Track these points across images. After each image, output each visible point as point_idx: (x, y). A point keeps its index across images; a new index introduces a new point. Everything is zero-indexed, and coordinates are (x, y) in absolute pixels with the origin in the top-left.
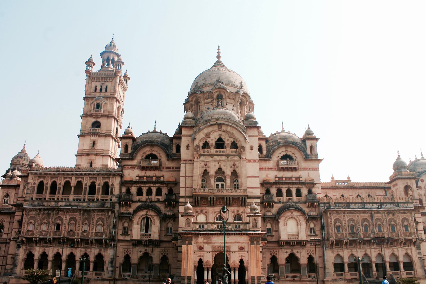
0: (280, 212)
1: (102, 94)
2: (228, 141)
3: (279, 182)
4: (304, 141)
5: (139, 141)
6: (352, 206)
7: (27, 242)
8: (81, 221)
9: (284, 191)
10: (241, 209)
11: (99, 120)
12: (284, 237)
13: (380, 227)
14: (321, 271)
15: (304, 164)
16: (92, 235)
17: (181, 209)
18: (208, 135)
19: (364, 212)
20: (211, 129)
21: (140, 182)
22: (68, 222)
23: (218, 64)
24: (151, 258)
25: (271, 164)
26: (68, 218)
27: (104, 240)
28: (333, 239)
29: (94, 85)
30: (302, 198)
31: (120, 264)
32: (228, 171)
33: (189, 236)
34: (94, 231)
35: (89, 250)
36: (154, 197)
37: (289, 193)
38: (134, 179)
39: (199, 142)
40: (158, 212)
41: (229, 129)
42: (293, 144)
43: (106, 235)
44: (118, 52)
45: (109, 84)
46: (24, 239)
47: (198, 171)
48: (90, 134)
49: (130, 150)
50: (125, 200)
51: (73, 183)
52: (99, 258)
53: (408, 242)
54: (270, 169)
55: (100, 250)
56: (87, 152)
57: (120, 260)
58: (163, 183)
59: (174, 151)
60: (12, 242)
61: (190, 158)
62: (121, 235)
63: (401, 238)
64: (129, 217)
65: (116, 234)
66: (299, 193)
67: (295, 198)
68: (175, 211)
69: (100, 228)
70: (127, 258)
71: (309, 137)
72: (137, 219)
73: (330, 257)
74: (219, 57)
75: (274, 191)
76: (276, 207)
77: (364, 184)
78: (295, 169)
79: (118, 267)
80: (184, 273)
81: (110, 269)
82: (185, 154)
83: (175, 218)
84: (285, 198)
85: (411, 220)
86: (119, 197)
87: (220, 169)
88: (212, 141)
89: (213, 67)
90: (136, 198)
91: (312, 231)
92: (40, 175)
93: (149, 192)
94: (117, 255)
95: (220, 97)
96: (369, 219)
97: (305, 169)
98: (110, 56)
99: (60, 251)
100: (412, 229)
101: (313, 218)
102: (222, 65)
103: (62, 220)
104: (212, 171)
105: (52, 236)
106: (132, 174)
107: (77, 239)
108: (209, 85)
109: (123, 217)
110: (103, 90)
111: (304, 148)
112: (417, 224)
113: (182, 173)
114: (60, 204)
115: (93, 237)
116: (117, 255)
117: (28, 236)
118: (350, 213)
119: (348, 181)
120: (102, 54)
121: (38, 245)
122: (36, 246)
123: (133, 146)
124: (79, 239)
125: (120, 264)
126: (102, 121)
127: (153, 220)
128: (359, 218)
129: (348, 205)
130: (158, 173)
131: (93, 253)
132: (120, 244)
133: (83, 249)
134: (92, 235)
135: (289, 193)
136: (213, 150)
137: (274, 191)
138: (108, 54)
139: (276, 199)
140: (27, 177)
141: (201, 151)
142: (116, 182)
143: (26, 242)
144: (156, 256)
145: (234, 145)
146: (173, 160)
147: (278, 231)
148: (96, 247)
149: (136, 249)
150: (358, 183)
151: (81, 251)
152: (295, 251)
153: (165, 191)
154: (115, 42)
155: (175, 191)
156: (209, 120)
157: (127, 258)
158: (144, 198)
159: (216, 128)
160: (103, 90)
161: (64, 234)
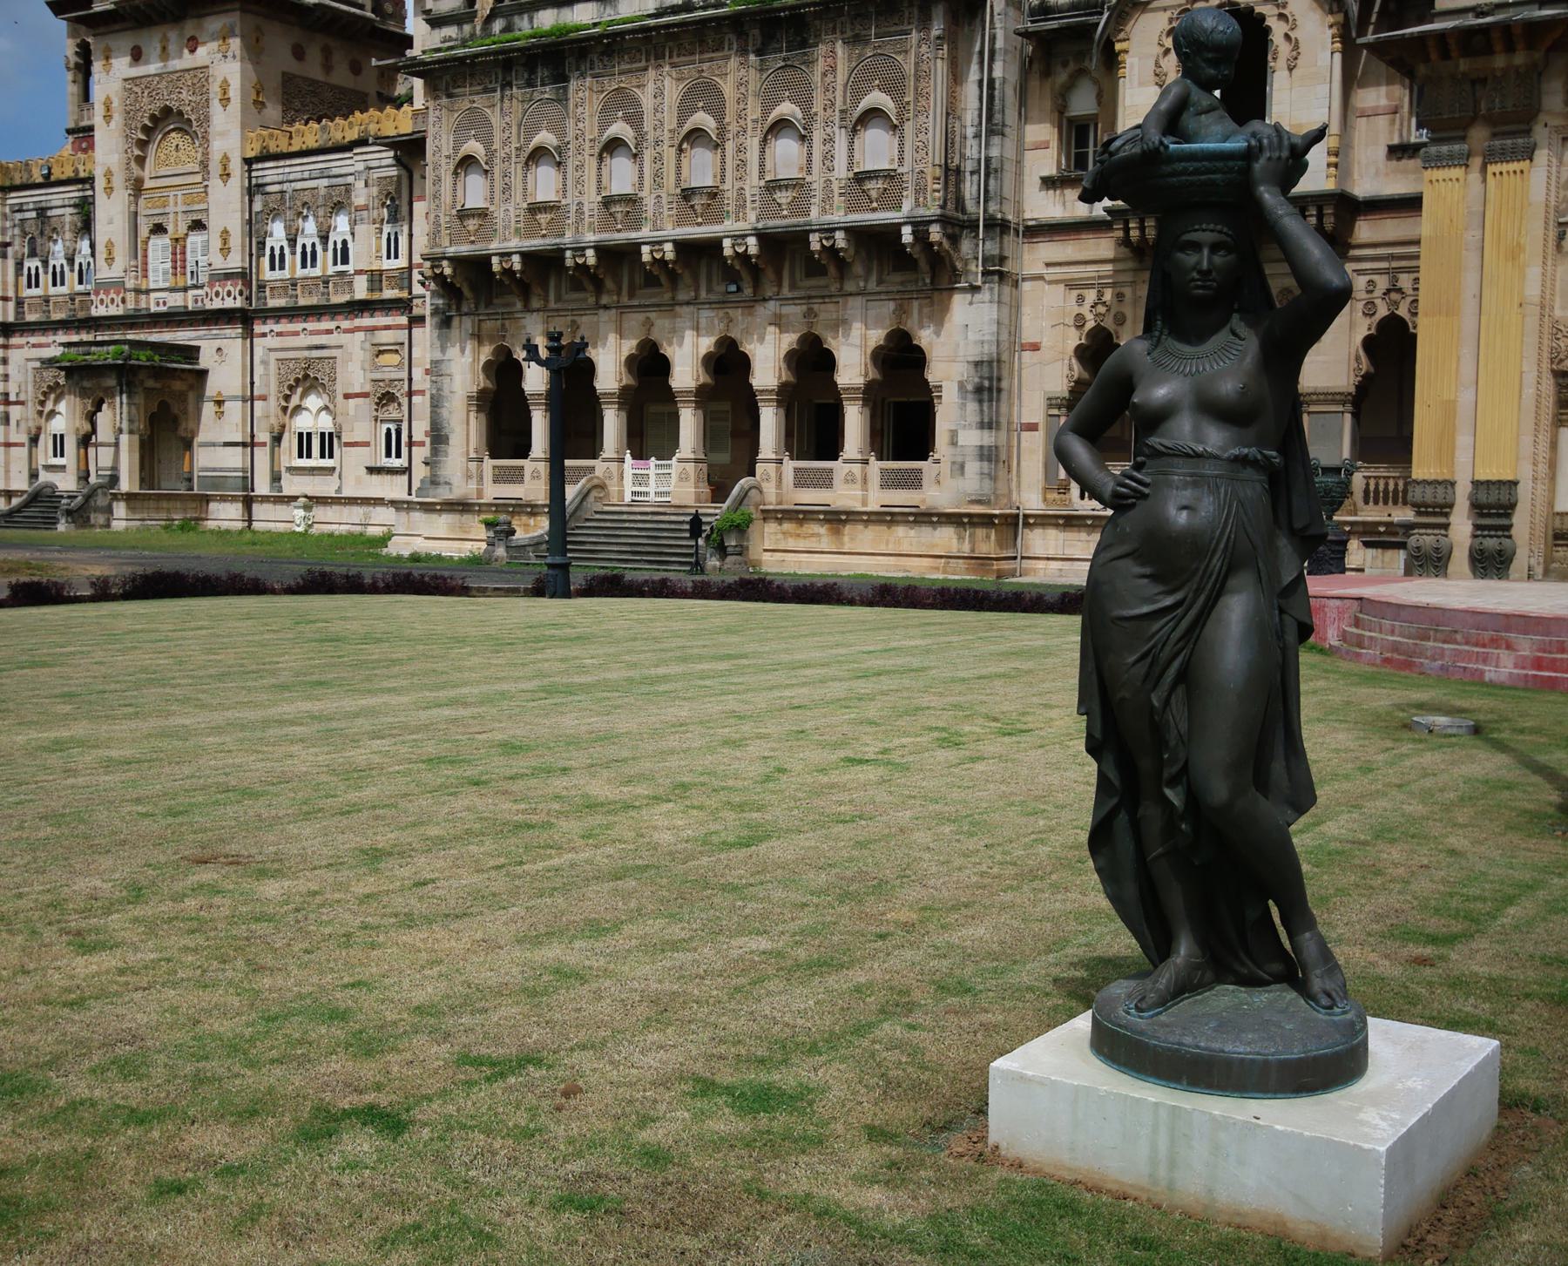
7: (473, 288)
8: (754, 111)
16: (827, 199)
22: (670, 121)
26: (673, 90)
27: (907, 231)
31: (1052, 402)
33: (1499, 61)
34: (841, 171)
35: (827, 312)
43: (920, 190)
46: (448, 271)
52: (901, 361)
55: (902, 311)
57: (1047, 375)
62: (1049, 183)
65: (1008, 177)
69: (877, 150)
79: (1033, 427)
80: (1446, 448)
81: (972, 438)
94: (1028, 336)
103: (635, 120)
105: (591, 237)
107: (740, 237)
115: (839, 216)
116: (1028, 336)
117: (464, 249)
121: (535, 303)
122: (527, 309)
124: (752, 241)
125: (1052, 402)
127: (1277, 29)
132: (1034, 258)
133: (794, 311)
134: (827, 199)
143: (467, 292)
148: (872, 286)
151: (779, 322)
161: (658, 214)
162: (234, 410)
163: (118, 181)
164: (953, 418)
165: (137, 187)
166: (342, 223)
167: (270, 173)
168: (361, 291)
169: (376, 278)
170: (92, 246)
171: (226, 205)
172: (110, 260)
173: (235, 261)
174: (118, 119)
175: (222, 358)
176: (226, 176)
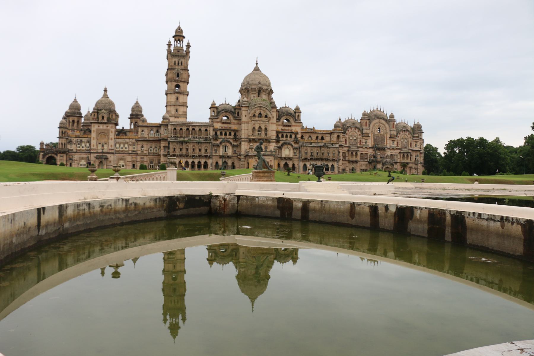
0: (282, 145)
1: (180, 68)
2: (264, 115)
3: (282, 132)
4: (295, 112)
5: (220, 109)
6: (313, 144)
9: (285, 135)
10: (267, 144)
11: (179, 84)
12: (283, 156)
13: (323, 154)
14: (297, 170)
15: (294, 124)
17: (243, 143)
18: (255, 111)
19: (318, 147)
20: (256, 109)
21: (221, 130)
23: (257, 69)
24: (227, 163)
25: (280, 123)
28: (303, 157)
29: (174, 60)
30: (292, 139)
32: (263, 128)
36: (228, 136)
37: (287, 136)
38: (219, 128)
39: (251, 115)
40: (231, 143)
41: (264, 109)
42: (290, 114)
44: (184, 35)
45: (183, 60)
47: (250, 128)
48: (175, 93)
49: (216, 114)
50: (216, 137)
51: (191, 129)
52: (206, 163)
53: (333, 160)
54: (279, 125)
56: (174, 104)
57: (214, 164)
58: (232, 130)
59: (236, 115)
60: (162, 156)
61: (246, 121)
63: (331, 158)
64: (218, 146)
66: (291, 137)
67: (289, 139)
68: (238, 143)
70: (217, 163)
71: (297, 111)
72: (221, 147)
73: (302, 164)
74: (257, 64)
75: (280, 135)
76: (281, 143)
77: (321, 131)
78: (290, 126)
82: (244, 119)
83: (239, 146)
84: (285, 139)
85: (336, 151)
86: (213, 136)
87: (260, 127)
88: (257, 114)
89: (254, 70)
90: (220, 136)
91: (295, 153)
92: (174, 125)
93: (226, 134)
95: (259, 91)
96: (319, 149)
97: (294, 126)
98: (179, 36)
99: (188, 160)
100: (336, 155)
101: (297, 148)
102: (259, 70)
104: (257, 128)
106: (218, 126)
108: (255, 84)
109: (214, 145)
110: (180, 64)
111: (294, 115)
112: (339, 152)
113: (243, 128)
114: (186, 139)
118: (311, 147)
119: (314, 129)
120: (173, 37)
123: (217, 111)
126: (181, 84)
128: (315, 150)
129: (311, 143)
130: (229, 125)
131: (203, 161)
132: (214, 157)
135: (287, 136)
136: (257, 119)
137: (280, 135)
138: (179, 37)
139: (281, 139)
140: (167, 125)
141: (253, 118)
142: (211, 130)
144: (230, 162)
145: (266, 116)
146: (236, 119)
147: (281, 153)
149: (221, 159)
150: (318, 130)
152: (287, 162)
153: (233, 134)
154: (182, 28)
155: (237, 134)
156: (256, 105)
157: (217, 163)
158: (223, 136)
159: (259, 108)
160: (180, 64)
162: (112, 162)
163: (95, 138)
164: (209, 166)
165: (97, 139)
166: (126, 146)
167: (117, 140)
168: (130, 152)
169: (133, 151)
170: (90, 145)
171: (111, 142)
172: (94, 146)
173: (113, 148)
174: (95, 133)
175: (111, 157)
176: (112, 139)
